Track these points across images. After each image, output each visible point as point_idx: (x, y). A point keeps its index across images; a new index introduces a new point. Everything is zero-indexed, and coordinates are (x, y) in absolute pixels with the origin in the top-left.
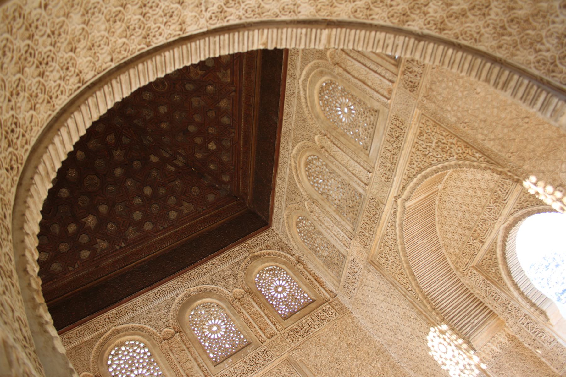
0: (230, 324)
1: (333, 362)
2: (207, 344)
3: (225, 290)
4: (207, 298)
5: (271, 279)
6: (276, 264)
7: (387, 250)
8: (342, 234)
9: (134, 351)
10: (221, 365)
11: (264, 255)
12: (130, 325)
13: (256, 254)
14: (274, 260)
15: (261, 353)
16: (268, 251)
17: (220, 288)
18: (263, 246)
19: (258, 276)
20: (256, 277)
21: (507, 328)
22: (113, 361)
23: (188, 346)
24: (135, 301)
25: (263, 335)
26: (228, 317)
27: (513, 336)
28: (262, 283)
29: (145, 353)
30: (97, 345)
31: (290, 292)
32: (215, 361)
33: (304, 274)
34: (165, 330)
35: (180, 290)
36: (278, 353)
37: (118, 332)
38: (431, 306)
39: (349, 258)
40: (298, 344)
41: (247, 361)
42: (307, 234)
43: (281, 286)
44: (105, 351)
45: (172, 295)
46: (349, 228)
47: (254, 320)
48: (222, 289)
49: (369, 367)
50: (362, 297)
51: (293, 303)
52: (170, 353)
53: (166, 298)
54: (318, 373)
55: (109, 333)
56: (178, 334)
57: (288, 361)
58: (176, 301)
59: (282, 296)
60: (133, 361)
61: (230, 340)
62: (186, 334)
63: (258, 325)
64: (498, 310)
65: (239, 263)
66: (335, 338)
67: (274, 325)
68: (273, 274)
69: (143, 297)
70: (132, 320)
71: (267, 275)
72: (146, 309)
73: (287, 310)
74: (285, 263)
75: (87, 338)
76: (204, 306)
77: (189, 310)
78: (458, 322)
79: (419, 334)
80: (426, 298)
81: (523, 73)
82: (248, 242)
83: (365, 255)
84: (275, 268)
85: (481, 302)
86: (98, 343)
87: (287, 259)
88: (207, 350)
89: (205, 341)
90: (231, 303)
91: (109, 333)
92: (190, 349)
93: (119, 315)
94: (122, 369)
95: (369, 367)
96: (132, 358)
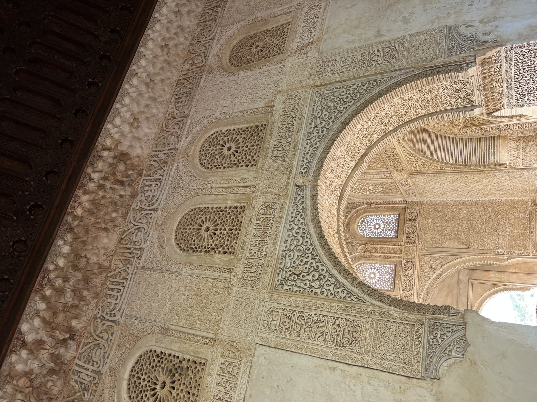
1: (442, 233)
2: (378, 286)
6: (360, 217)
7: (415, 163)
8: (382, 175)
10: (396, 288)
11: (350, 219)
14: (358, 216)
15: (406, 264)
19: (360, 231)
21: (510, 136)
25: (397, 255)
27: (517, 137)
31: (383, 222)
33: (379, 207)
36: (413, 256)
38: (463, 165)
39: (397, 181)
40: (417, 242)
42: (361, 189)
43: (376, 224)
46: (384, 170)
47: (384, 253)
49: (461, 217)
50: (422, 191)
51: (391, 226)
54: (441, 245)
61: (386, 273)
64: (497, 133)
66: (430, 221)
68: (365, 223)
71: (363, 226)
73: (393, 232)
74: (364, 212)
78: (484, 159)
79: (470, 181)
80: (456, 165)
81: (446, 111)
83: (405, 174)
85: (485, 138)
87: (363, 209)
95: (461, 217)
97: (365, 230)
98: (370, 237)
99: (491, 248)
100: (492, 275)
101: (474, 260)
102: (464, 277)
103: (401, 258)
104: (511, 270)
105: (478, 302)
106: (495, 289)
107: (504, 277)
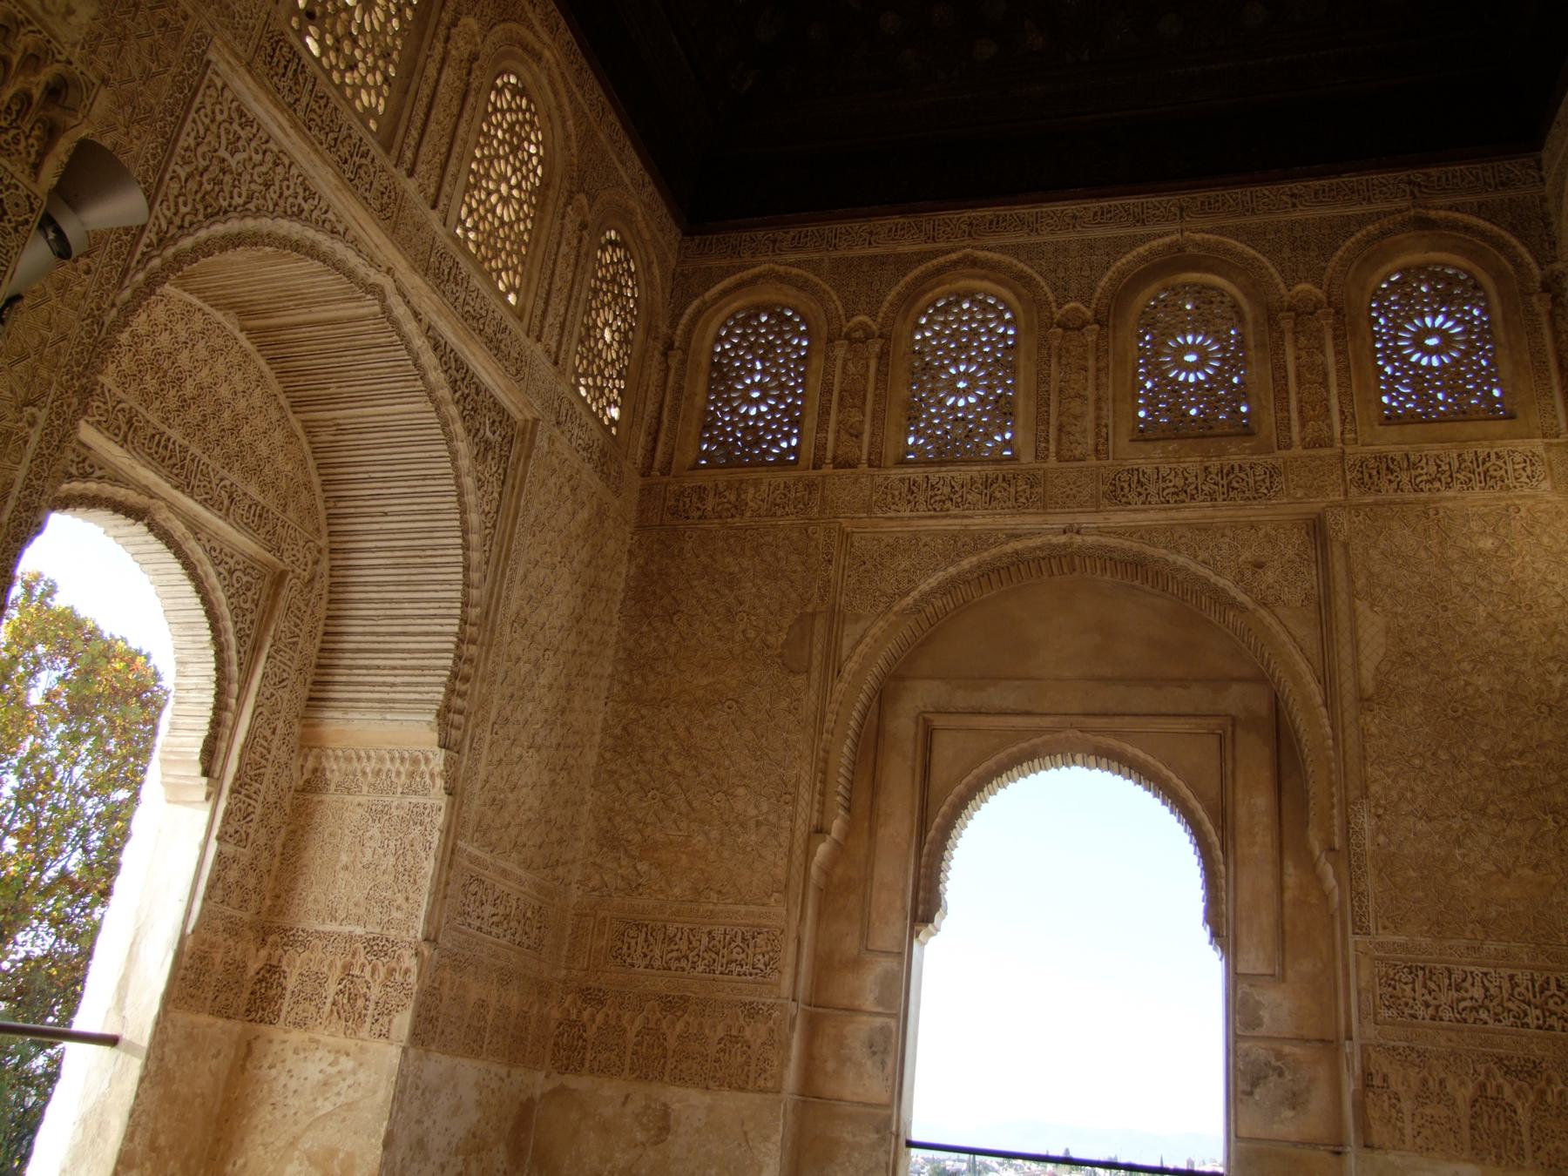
2: (1149, 385)
3: (1276, 275)
4: (1219, 274)
5: (1426, 304)
9: (984, 322)
10: (1148, 447)
11: (1454, 226)
12: (1007, 259)
13: (1432, 214)
15: (1259, 470)
16: (1474, 220)
17: (1268, 264)
18: (1470, 199)
20: (1386, 279)
22: (930, 322)
23: (1102, 364)
24: (1047, 208)
25: (1295, 429)
26: (1241, 344)
28: (1393, 303)
29: (1004, 336)
30: (916, 272)
32: (1141, 431)
34: (1072, 304)
35: (1167, 228)
37: (974, 263)
40: (1369, 499)
41: (1213, 470)
44: (925, 292)
45: (1140, 230)
48: (1272, 270)
52: (1054, 360)
53: (1122, 232)
55: (954, 256)
56: (1096, 327)
57: (1317, 529)
58: (1141, 249)
60: (970, 341)
62: (1115, 338)
63: (1300, 401)
65: (1362, 221)
67: (1343, 422)
69: (1070, 208)
70: (1015, 250)
72: (1061, 237)
74: (1499, 276)
75: (907, 248)
76: (1200, 291)
77: (1155, 286)
82: (1434, 171)
86: (922, 268)
88: (1140, 396)
89: (1148, 376)
90: (1270, 317)
91: (954, 256)
92: (1102, 374)
93: (994, 226)
96: (974, 334)
98: (1376, 321)
99: (1374, 788)
100: (1262, 801)
101: (1312, 725)
102: (1235, 699)
103: (1289, 447)
104: (1290, 868)
105: (1142, 755)
106: (1202, 815)
107: (1257, 841)
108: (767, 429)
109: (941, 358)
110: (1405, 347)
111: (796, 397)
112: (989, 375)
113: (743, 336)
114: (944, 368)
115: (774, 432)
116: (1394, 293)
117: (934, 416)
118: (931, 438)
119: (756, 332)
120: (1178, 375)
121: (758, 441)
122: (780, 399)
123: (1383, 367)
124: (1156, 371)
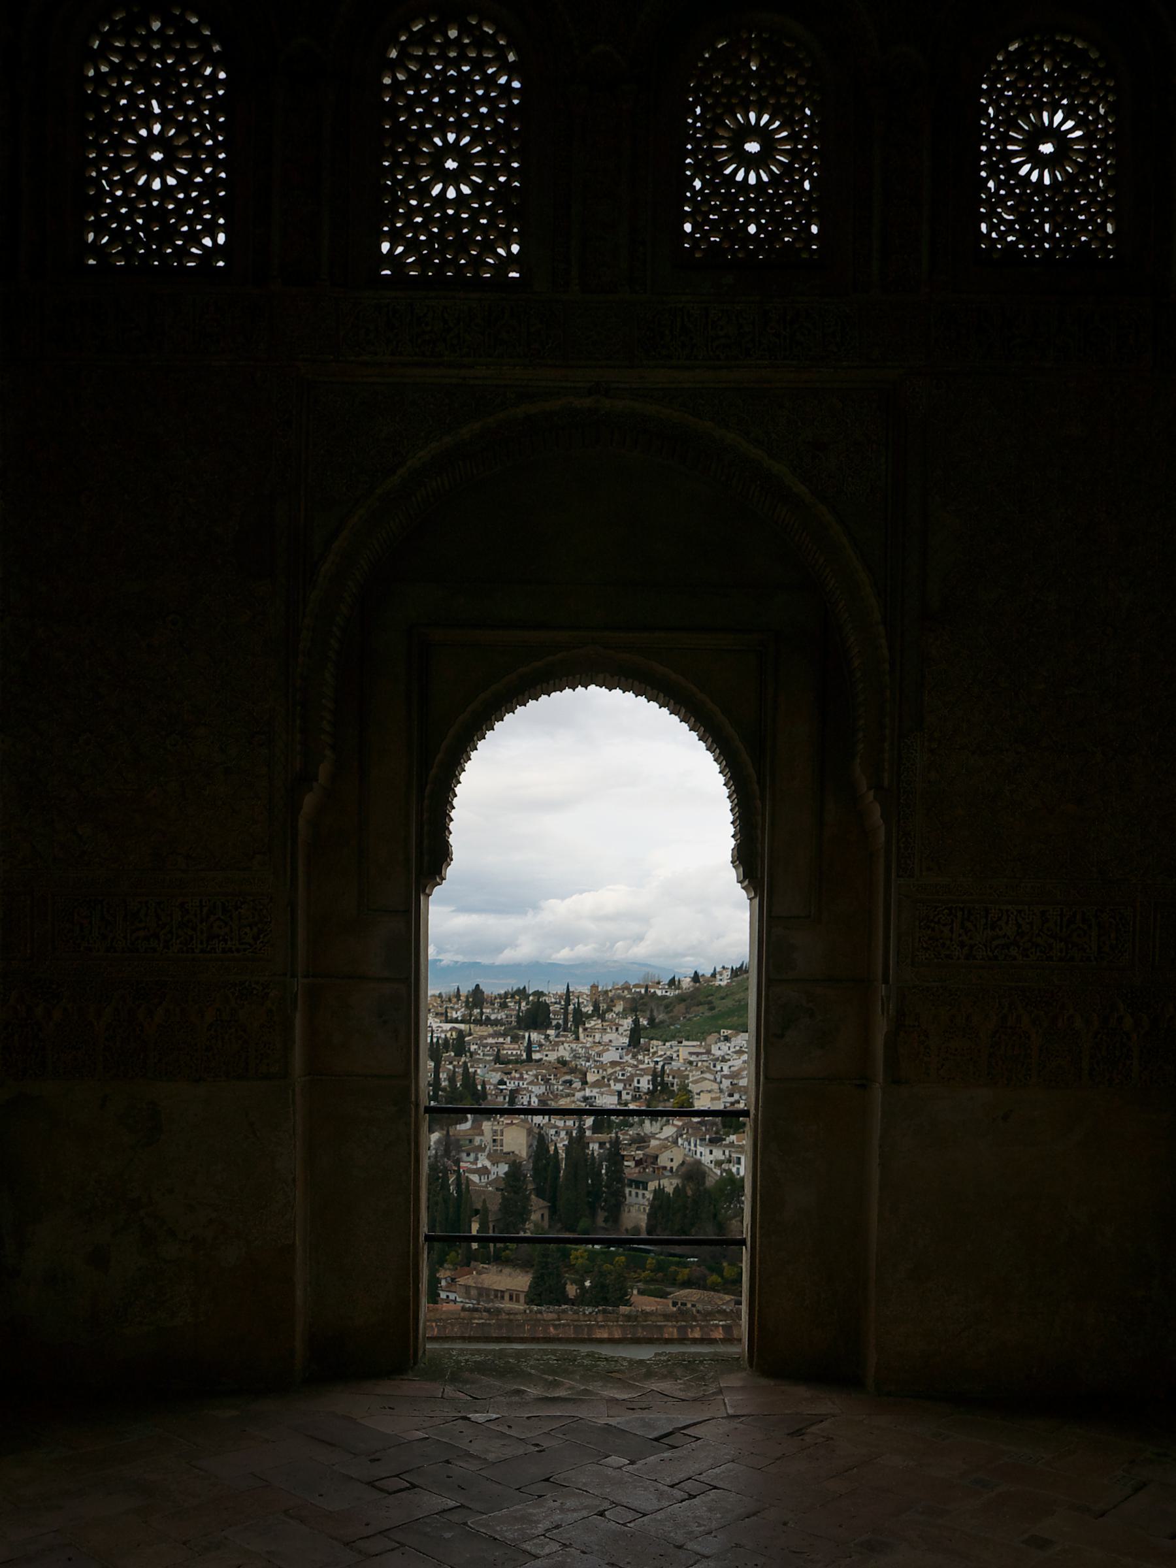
0: (806, 163)
2: (698, 184)
5: (1045, 92)
28: (1008, 86)
59: (1034, 177)
84: (1094, 55)
89: (699, 170)
94: (418, 99)
97: (1024, 76)
108: (179, 212)
109: (421, 119)
110: (1015, 154)
111: (218, 165)
112: (487, 153)
113: (128, 54)
114: (427, 136)
115: (190, 221)
116: (1010, 70)
117: (412, 212)
118: (413, 246)
119: (146, 48)
120: (735, 172)
121: (170, 233)
122: (195, 166)
123: (987, 180)
124: (709, 166)
